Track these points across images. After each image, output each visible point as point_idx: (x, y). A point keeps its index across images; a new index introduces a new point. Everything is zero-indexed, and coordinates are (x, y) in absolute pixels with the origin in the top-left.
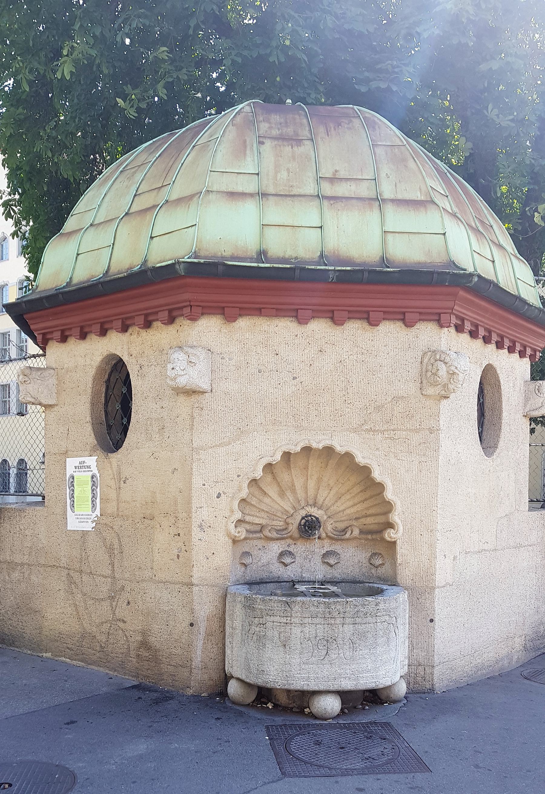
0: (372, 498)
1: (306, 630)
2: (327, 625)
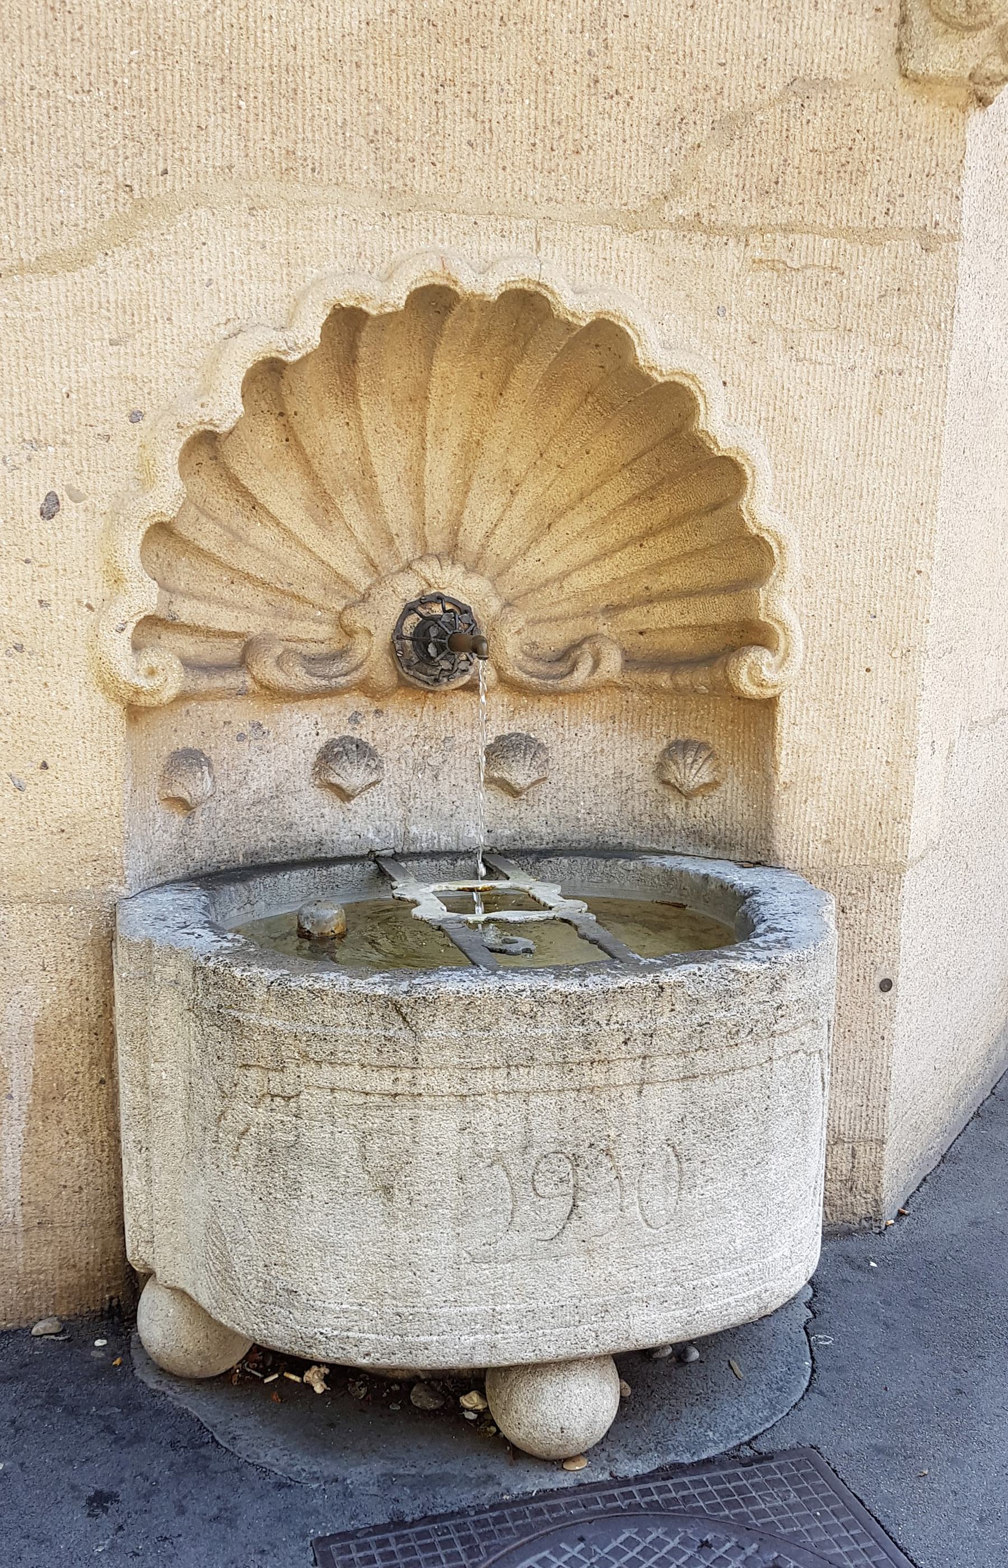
0: (680, 524)
1: (485, 1120)
2: (574, 1094)
